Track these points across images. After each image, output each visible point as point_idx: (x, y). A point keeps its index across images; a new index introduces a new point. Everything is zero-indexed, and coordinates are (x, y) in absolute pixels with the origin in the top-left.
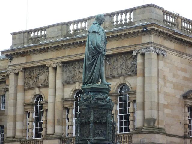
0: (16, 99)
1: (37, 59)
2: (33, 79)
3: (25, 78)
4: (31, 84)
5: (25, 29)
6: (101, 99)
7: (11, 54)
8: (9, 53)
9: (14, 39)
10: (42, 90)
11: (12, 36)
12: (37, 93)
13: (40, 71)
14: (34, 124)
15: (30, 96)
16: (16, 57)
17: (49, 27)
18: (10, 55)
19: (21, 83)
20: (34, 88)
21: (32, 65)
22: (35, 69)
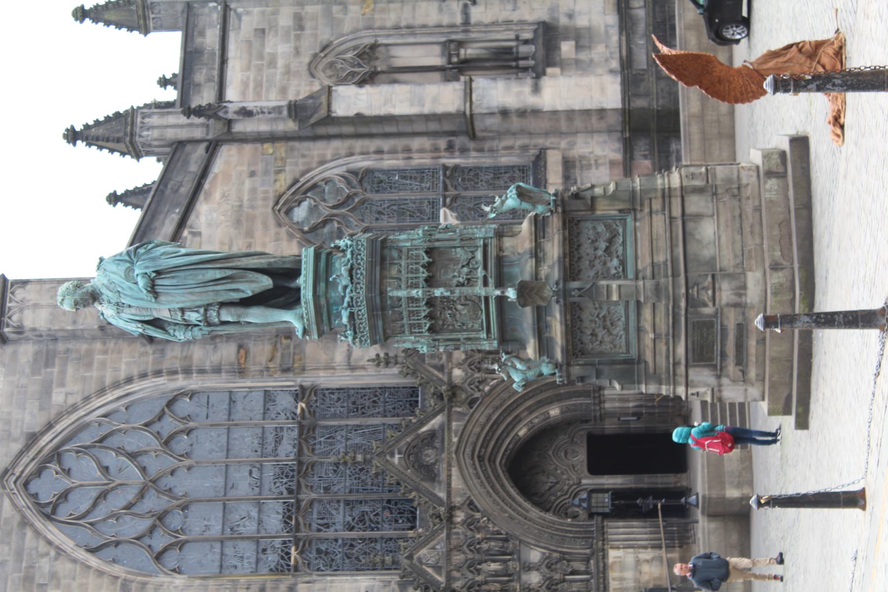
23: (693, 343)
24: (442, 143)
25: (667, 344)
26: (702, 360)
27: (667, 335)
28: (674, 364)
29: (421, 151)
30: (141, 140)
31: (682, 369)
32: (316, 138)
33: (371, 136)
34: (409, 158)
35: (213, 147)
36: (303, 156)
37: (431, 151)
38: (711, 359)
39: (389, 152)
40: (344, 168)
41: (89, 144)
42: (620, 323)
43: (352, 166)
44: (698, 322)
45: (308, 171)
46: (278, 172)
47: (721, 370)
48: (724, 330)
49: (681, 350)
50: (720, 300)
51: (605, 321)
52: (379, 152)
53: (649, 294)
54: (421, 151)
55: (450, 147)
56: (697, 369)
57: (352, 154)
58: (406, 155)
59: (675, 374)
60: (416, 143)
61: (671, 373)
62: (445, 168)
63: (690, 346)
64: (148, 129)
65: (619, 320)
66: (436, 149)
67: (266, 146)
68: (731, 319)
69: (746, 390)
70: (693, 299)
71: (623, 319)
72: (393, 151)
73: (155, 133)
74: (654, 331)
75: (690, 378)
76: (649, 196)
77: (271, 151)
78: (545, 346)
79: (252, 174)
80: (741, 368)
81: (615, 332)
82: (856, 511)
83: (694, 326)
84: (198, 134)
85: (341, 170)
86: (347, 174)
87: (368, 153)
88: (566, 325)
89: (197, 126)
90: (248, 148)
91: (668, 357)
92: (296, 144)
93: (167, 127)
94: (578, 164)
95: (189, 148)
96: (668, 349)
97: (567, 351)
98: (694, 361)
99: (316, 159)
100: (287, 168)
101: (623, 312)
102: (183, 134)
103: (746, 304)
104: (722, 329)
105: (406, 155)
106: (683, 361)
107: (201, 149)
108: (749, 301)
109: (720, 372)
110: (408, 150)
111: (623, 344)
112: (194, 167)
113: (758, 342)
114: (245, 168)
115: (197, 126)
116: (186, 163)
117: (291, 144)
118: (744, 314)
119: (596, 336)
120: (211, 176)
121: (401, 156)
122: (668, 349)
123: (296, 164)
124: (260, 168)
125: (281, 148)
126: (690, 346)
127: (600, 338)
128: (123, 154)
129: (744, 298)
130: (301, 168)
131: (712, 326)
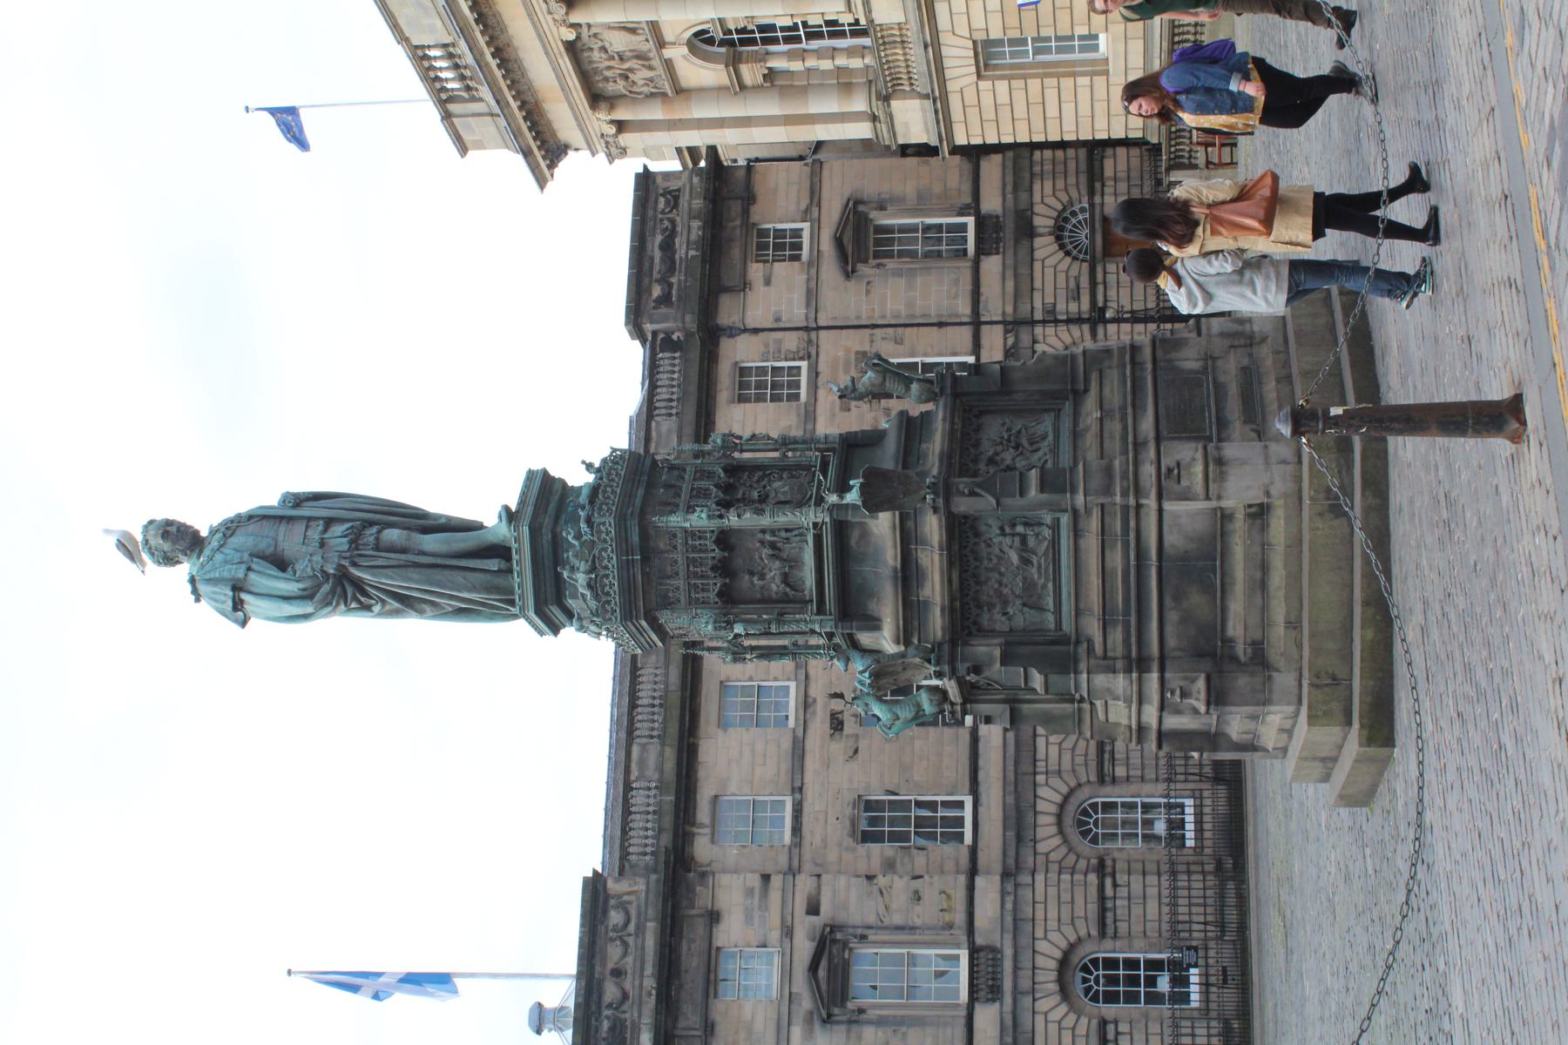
0: (720, 123)
1: (546, 72)
2: (631, 70)
3: (632, 97)
4: (650, 74)
5: (432, 113)
6: (593, 569)
7: (544, 158)
8: (543, 164)
9: (480, 146)
10: (669, 37)
11: (470, 153)
12: (685, 50)
13: (591, 49)
14: (815, 44)
15: (700, 73)
16: (554, 134)
17: (402, 38)
18: (544, 150)
19: (655, 112)
20: (669, 65)
21: (573, 81)
22: (588, 67)
25: (1123, 419)
27: (1123, 408)
28: (1135, 444)
48: (1220, 389)
49: (1147, 425)
68: (1230, 369)
69: (1266, 447)
71: (1051, 438)
74: (1101, 408)
78: (912, 613)
82: (1500, 446)
88: (950, 556)
91: (1124, 438)
97: (952, 610)
106: (1152, 435)
108: (1256, 328)
113: (1278, 381)
118: (1250, 355)
122: (1125, 428)
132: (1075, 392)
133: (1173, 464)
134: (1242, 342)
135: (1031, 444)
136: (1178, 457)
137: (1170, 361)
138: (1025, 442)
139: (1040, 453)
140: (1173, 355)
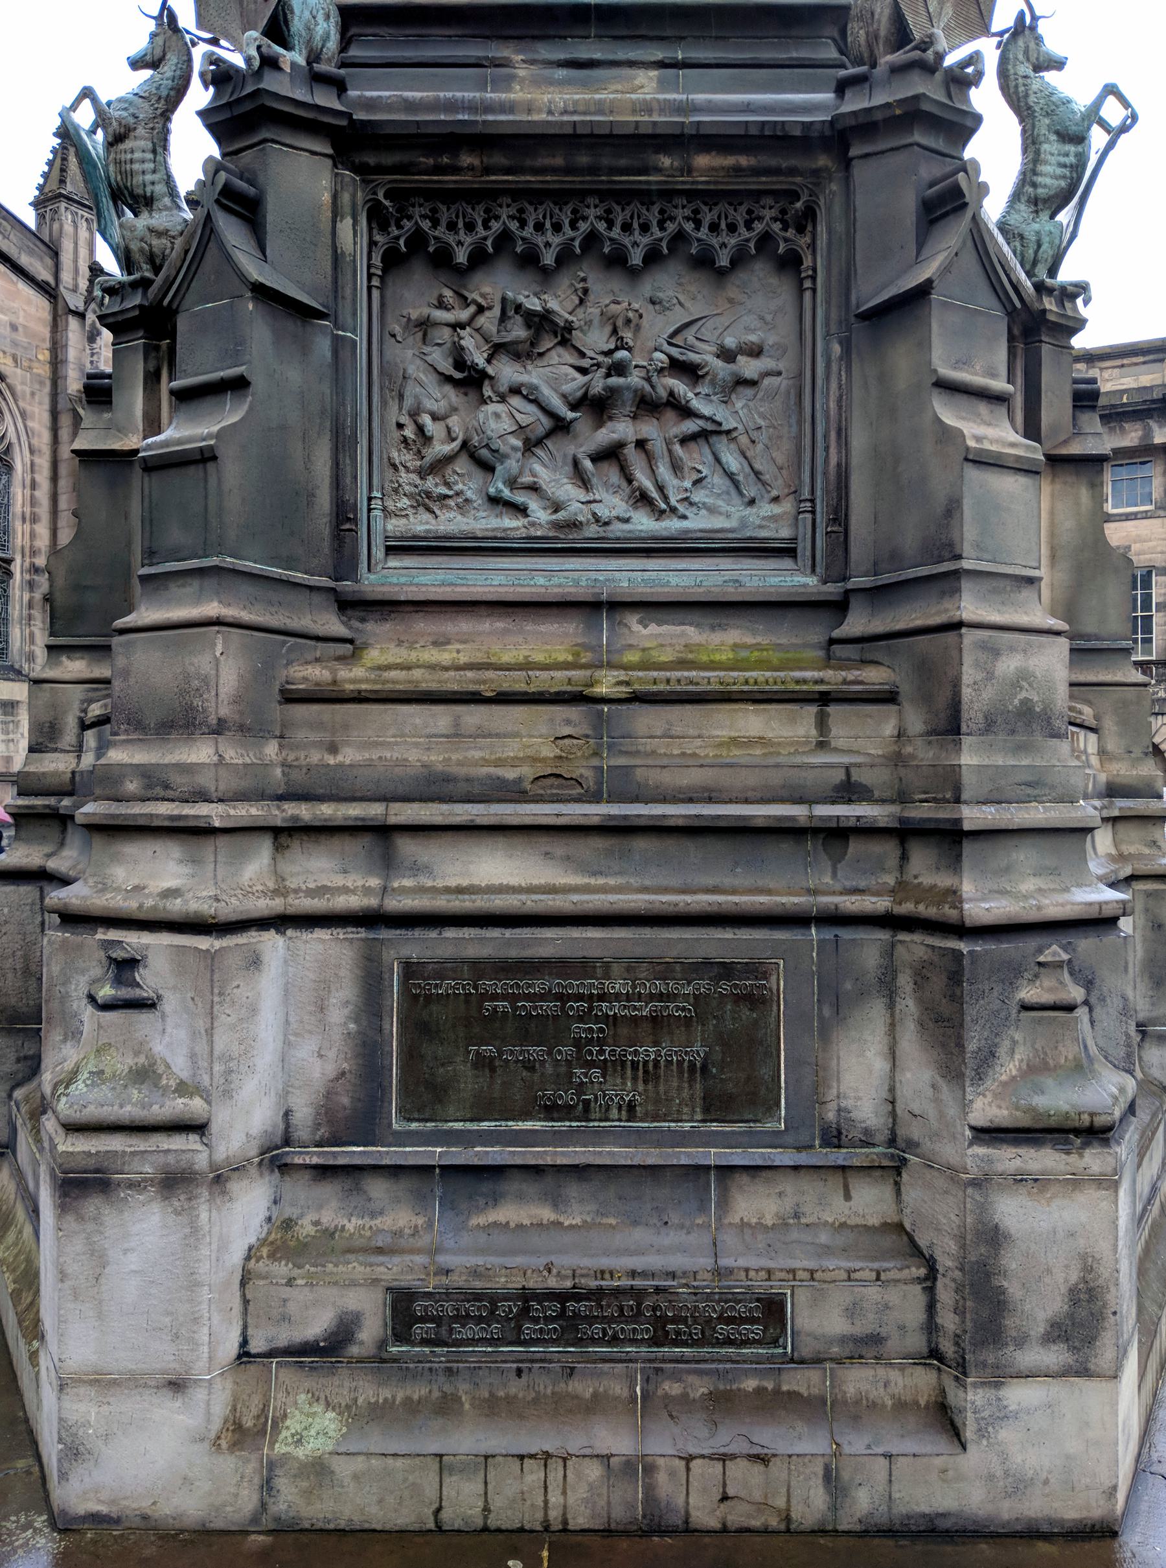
23: (583, 967)
24: (41, 561)
25: (554, 782)
26: (420, 1028)
28: (384, 832)
29: (33, 535)
30: (63, 209)
31: (330, 877)
32: (55, 414)
33: (54, 478)
34: (24, 520)
35: (49, 291)
36: (33, 394)
37: (31, 547)
38: (427, 1095)
39: (32, 496)
40: (14, 440)
41: (54, 151)
42: (612, 503)
43: (16, 449)
44: (757, 1001)
45: (13, 394)
46: (15, 358)
47: (324, 1171)
49: (497, 872)
50: (1035, 1183)
51: (648, 406)
52: (34, 485)
53: (1008, 665)
54: (33, 535)
55: (35, 570)
56: (343, 998)
57: (32, 452)
58: (28, 516)
59: (283, 835)
60: (43, 530)
61: (304, 812)
62: (9, 561)
63: (551, 943)
64: (74, 222)
65: (642, 499)
66: (34, 553)
67: (47, 353)
70: (1013, 973)
71: (644, 523)
72: (33, 502)
73: (68, 228)
75: (272, 944)
76: (1109, 724)
77: (40, 357)
79: (14, 327)
80: (370, 1332)
81: (541, 471)
83: (726, 970)
84: (66, 277)
85: (11, 435)
86: (6, 442)
87: (32, 471)
89: (75, 279)
90: (46, 332)
91: (435, 787)
92: (47, 389)
93: (76, 244)
94: (10, 718)
95: (49, 262)
96: (516, 793)
98: (410, 969)
99: (28, 408)
100: (19, 371)
101: (697, 522)
102: (66, 258)
103: (999, 1377)
104: (700, 1170)
105: (28, 516)
107: (45, 275)
108: (1018, 1395)
109: (324, 1152)
110: (34, 519)
111: (449, 522)
112: (24, 260)
114: (21, 320)
115: (75, 279)
116: (31, 253)
117: (48, 383)
119: (521, 353)
120: (14, 277)
121: (28, 510)
123: (23, 383)
124: (20, 337)
125: (44, 371)
126: (551, 943)
127: (507, 372)
128: (41, 188)
129: (1055, 1356)
130: (19, 388)
131: (717, 1106)
132: (839, 607)
133: (149, 979)
134: (948, 1320)
135: (611, 454)
136: (170, 1003)
137: (888, 987)
138: (621, 429)
139: (569, 492)
140: (908, 1004)
